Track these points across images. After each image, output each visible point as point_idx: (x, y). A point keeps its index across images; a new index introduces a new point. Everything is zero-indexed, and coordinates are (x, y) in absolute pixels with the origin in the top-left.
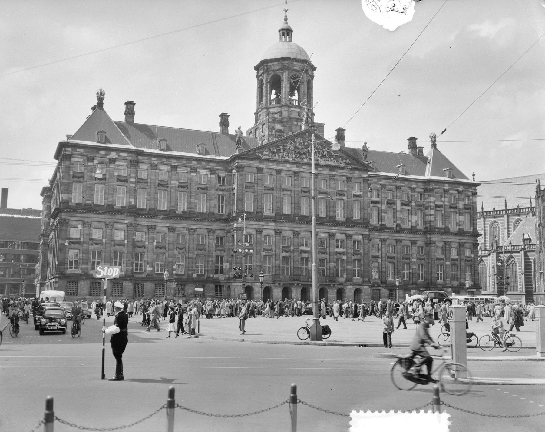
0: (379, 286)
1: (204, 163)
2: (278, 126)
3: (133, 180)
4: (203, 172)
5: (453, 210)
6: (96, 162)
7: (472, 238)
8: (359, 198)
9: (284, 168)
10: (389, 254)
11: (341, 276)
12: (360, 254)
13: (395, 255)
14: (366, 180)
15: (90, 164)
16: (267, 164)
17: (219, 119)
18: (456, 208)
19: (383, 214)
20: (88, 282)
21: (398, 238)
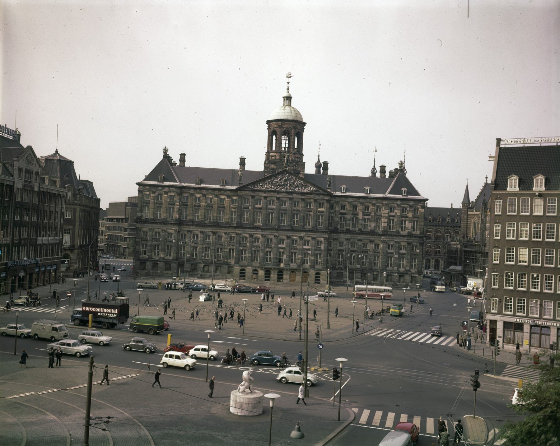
0: (342, 270)
1: (223, 192)
2: (272, 166)
3: (178, 204)
4: (223, 197)
5: (404, 219)
6: (157, 194)
7: (418, 239)
8: (322, 214)
9: (269, 195)
10: (351, 249)
11: (307, 263)
12: (321, 250)
13: (355, 249)
14: (328, 201)
15: (153, 195)
16: (258, 193)
17: (239, 161)
18: (407, 217)
19: (348, 222)
20: (151, 263)
21: (359, 238)
